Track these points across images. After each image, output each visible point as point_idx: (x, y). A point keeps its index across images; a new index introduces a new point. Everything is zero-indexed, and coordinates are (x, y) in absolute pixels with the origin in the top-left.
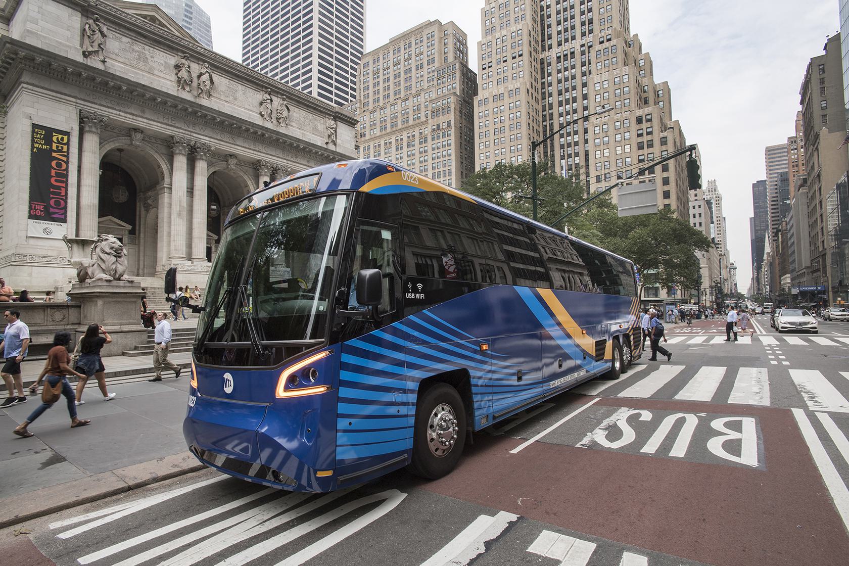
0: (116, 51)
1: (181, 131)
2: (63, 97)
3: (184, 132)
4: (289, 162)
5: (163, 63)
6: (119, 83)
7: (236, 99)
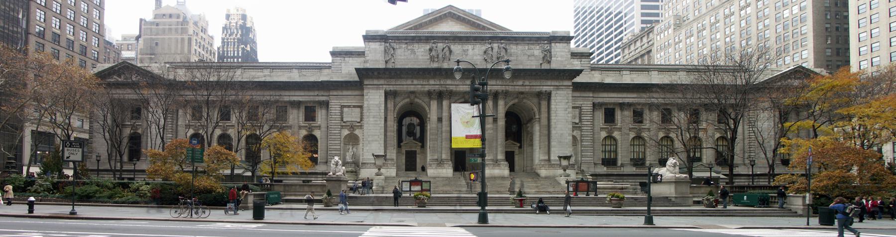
5: (423, 50)
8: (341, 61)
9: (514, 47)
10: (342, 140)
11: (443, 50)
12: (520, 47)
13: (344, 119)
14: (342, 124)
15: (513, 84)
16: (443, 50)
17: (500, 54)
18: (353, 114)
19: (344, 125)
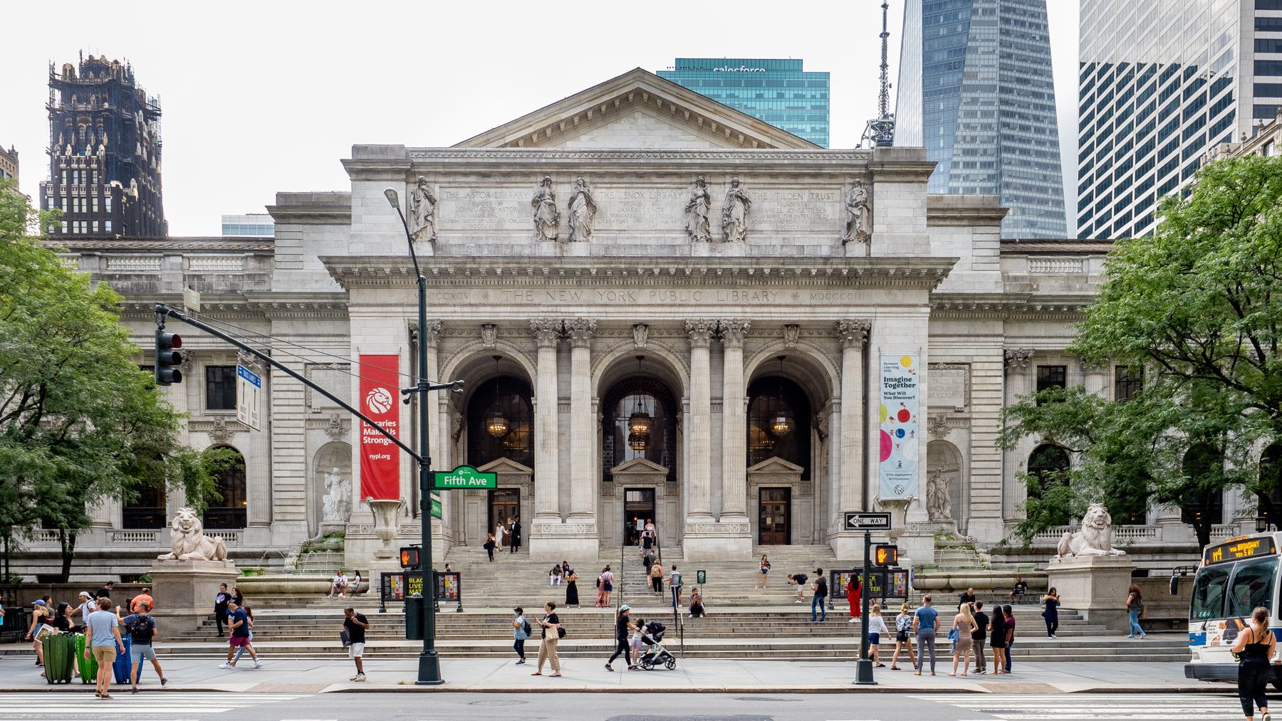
0: (453, 216)
1: (541, 309)
2: (389, 309)
3: (545, 309)
4: (748, 309)
5: (516, 205)
6: (443, 266)
7: (639, 220)
9: (770, 194)
11: (570, 205)
12: (787, 194)
15: (765, 302)
16: (570, 205)
17: (729, 216)
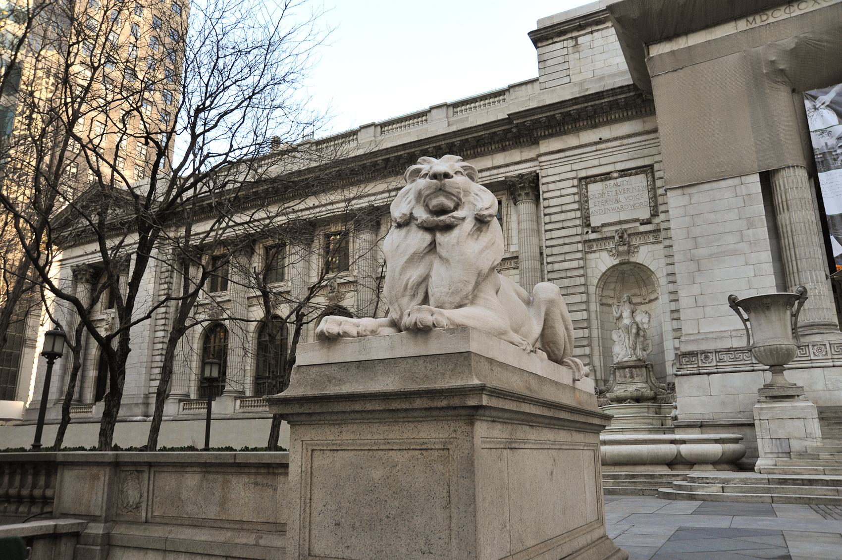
8: (565, 51)
10: (592, 289)
13: (592, 219)
14: (586, 237)
18: (621, 197)
19: (597, 240)
